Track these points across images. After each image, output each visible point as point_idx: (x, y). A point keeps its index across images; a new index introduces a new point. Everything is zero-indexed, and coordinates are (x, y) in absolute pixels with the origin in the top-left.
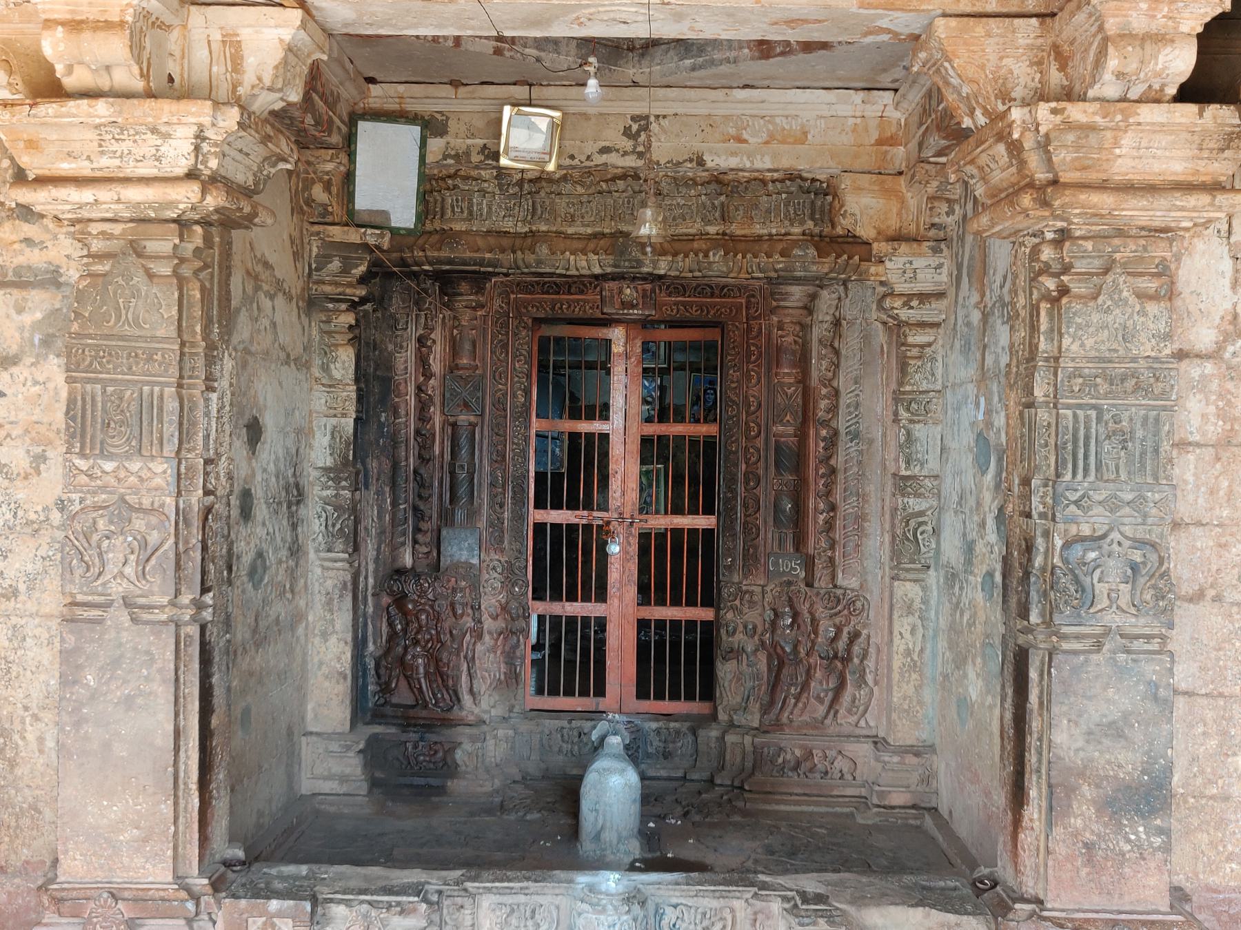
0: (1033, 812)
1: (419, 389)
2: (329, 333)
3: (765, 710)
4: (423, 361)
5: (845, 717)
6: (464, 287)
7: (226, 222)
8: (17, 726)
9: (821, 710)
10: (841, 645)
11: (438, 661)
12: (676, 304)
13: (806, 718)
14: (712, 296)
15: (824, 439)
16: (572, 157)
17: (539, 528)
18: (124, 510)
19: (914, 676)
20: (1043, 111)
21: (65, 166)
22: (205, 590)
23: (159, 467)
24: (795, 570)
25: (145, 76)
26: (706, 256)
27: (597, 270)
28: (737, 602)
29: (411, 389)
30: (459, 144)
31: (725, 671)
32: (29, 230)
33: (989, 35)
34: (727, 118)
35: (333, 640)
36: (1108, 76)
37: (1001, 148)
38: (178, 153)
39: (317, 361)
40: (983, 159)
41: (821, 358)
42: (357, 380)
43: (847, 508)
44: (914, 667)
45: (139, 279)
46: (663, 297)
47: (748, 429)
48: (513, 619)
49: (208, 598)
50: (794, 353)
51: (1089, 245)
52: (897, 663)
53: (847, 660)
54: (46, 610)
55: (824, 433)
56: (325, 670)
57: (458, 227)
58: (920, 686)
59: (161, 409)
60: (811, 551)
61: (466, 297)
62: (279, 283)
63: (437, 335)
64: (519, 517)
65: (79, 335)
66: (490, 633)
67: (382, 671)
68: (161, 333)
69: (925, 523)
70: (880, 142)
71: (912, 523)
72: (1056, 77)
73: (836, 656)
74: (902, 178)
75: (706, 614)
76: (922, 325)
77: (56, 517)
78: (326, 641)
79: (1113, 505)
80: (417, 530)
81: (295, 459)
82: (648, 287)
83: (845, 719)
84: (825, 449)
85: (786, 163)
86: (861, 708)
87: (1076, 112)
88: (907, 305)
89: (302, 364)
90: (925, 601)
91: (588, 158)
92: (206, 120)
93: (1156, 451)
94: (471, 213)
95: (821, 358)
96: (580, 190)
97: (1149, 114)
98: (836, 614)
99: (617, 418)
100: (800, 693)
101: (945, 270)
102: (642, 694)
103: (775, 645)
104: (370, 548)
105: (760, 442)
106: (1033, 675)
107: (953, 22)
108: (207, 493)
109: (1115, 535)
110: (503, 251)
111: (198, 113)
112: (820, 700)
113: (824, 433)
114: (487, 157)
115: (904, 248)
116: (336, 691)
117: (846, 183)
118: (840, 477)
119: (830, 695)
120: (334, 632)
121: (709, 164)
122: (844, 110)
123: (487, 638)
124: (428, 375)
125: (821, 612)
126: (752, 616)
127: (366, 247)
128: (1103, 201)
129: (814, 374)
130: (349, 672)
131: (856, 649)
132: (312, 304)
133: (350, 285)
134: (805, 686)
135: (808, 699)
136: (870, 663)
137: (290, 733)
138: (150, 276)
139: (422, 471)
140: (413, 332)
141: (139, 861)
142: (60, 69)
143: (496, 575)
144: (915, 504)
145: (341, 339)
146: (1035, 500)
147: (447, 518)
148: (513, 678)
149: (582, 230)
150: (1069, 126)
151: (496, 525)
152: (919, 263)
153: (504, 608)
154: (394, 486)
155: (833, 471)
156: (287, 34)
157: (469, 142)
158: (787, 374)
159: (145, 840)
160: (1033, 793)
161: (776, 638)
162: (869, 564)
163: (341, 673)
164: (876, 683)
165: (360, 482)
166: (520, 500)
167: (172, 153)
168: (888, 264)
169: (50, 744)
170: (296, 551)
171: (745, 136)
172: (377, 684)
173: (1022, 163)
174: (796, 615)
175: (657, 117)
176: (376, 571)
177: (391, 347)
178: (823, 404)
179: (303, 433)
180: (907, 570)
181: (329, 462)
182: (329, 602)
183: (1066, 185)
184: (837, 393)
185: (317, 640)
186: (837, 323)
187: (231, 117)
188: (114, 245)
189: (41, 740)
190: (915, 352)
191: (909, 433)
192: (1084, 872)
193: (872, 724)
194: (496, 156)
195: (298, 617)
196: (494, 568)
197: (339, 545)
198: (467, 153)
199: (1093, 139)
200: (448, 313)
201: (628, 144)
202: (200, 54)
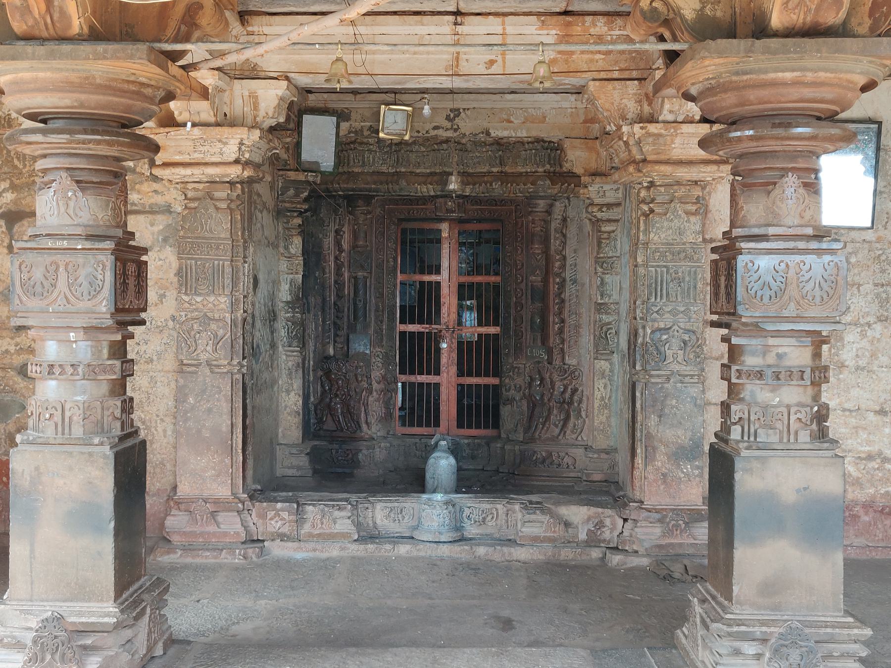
0: (639, 460)
1: (336, 258)
2: (288, 229)
3: (526, 431)
4: (338, 243)
6: (360, 202)
7: (250, 181)
8: (153, 424)
9: (557, 431)
10: (567, 395)
11: (348, 406)
12: (476, 210)
13: (548, 435)
14: (496, 205)
15: (558, 284)
16: (418, 132)
17: (403, 334)
18: (206, 320)
19: (606, 411)
20: (637, 127)
21: (177, 157)
22: (244, 358)
23: (223, 299)
25: (215, 116)
26: (491, 185)
27: (432, 193)
28: (511, 374)
29: (332, 258)
30: (357, 125)
31: (505, 411)
32: (156, 186)
33: (614, 89)
34: (502, 109)
35: (293, 394)
36: (665, 112)
37: (621, 143)
38: (231, 152)
39: (282, 244)
40: (616, 147)
41: (556, 239)
42: (303, 254)
43: (570, 321)
44: (605, 406)
45: (212, 210)
46: (469, 207)
47: (517, 278)
49: (245, 363)
50: (541, 236)
51: (662, 189)
52: (596, 405)
53: (570, 403)
54: (166, 369)
55: (558, 280)
56: (288, 410)
57: (356, 170)
58: (610, 417)
59: (223, 272)
60: (551, 345)
61: (362, 208)
62: (264, 204)
63: (345, 229)
64: (392, 328)
65: (183, 237)
66: (376, 391)
67: (318, 412)
68: (223, 236)
69: (611, 328)
70: (585, 122)
71: (604, 329)
72: (647, 109)
73: (564, 402)
74: (598, 142)
75: (494, 381)
76: (609, 221)
77: (171, 324)
79: (674, 313)
80: (336, 335)
81: (272, 297)
82: (461, 201)
83: (570, 436)
84: (558, 289)
85: (534, 133)
87: (653, 128)
88: (600, 210)
89: (275, 246)
90: (611, 371)
91: (427, 132)
92: (245, 136)
93: (695, 287)
94: (364, 162)
95: (556, 239)
96: (423, 149)
97: (686, 128)
99: (445, 273)
100: (545, 422)
101: (620, 191)
102: (460, 425)
103: (531, 395)
104: (311, 345)
105: (523, 286)
106: (638, 394)
107: (597, 83)
108: (245, 312)
109: (676, 327)
110: (381, 183)
111: (241, 133)
112: (557, 426)
113: (558, 280)
114: (372, 132)
115: (598, 179)
117: (567, 144)
118: (567, 304)
119: (562, 423)
121: (493, 135)
122: (565, 104)
123: (375, 393)
124: (341, 250)
125: (556, 377)
126: (519, 381)
127: (308, 182)
128: (667, 169)
129: (553, 248)
130: (301, 411)
131: (576, 398)
132: (279, 213)
133: (299, 203)
134: (548, 418)
136: (584, 406)
137: (272, 443)
138: (217, 209)
139: (338, 303)
140: (333, 227)
141: (215, 486)
142: (176, 114)
144: (605, 318)
145: (294, 232)
146: (638, 311)
147: (352, 328)
148: (389, 415)
149: (424, 171)
150: (649, 135)
151: (379, 332)
152: (606, 187)
154: (323, 310)
155: (563, 301)
156: (280, 93)
157: (362, 124)
158: (537, 248)
159: (218, 476)
160: (639, 451)
162: (582, 351)
165: (305, 309)
166: (392, 319)
167: (228, 151)
168: (590, 189)
169: (169, 433)
170: (273, 346)
171: (512, 119)
173: (630, 151)
174: (542, 380)
175: (464, 109)
176: (314, 357)
177: (321, 236)
178: (557, 264)
179: (276, 283)
180: (602, 354)
181: (289, 298)
182: (290, 374)
183: (650, 162)
184: (564, 258)
185: (284, 394)
186: (564, 220)
187: (257, 133)
188: (199, 194)
189: (165, 431)
190: (605, 236)
191: (602, 280)
192: (662, 487)
194: (377, 132)
195: (274, 382)
197: (295, 343)
198: (362, 130)
199: (661, 140)
200: (351, 217)
201: (449, 125)
202: (239, 102)
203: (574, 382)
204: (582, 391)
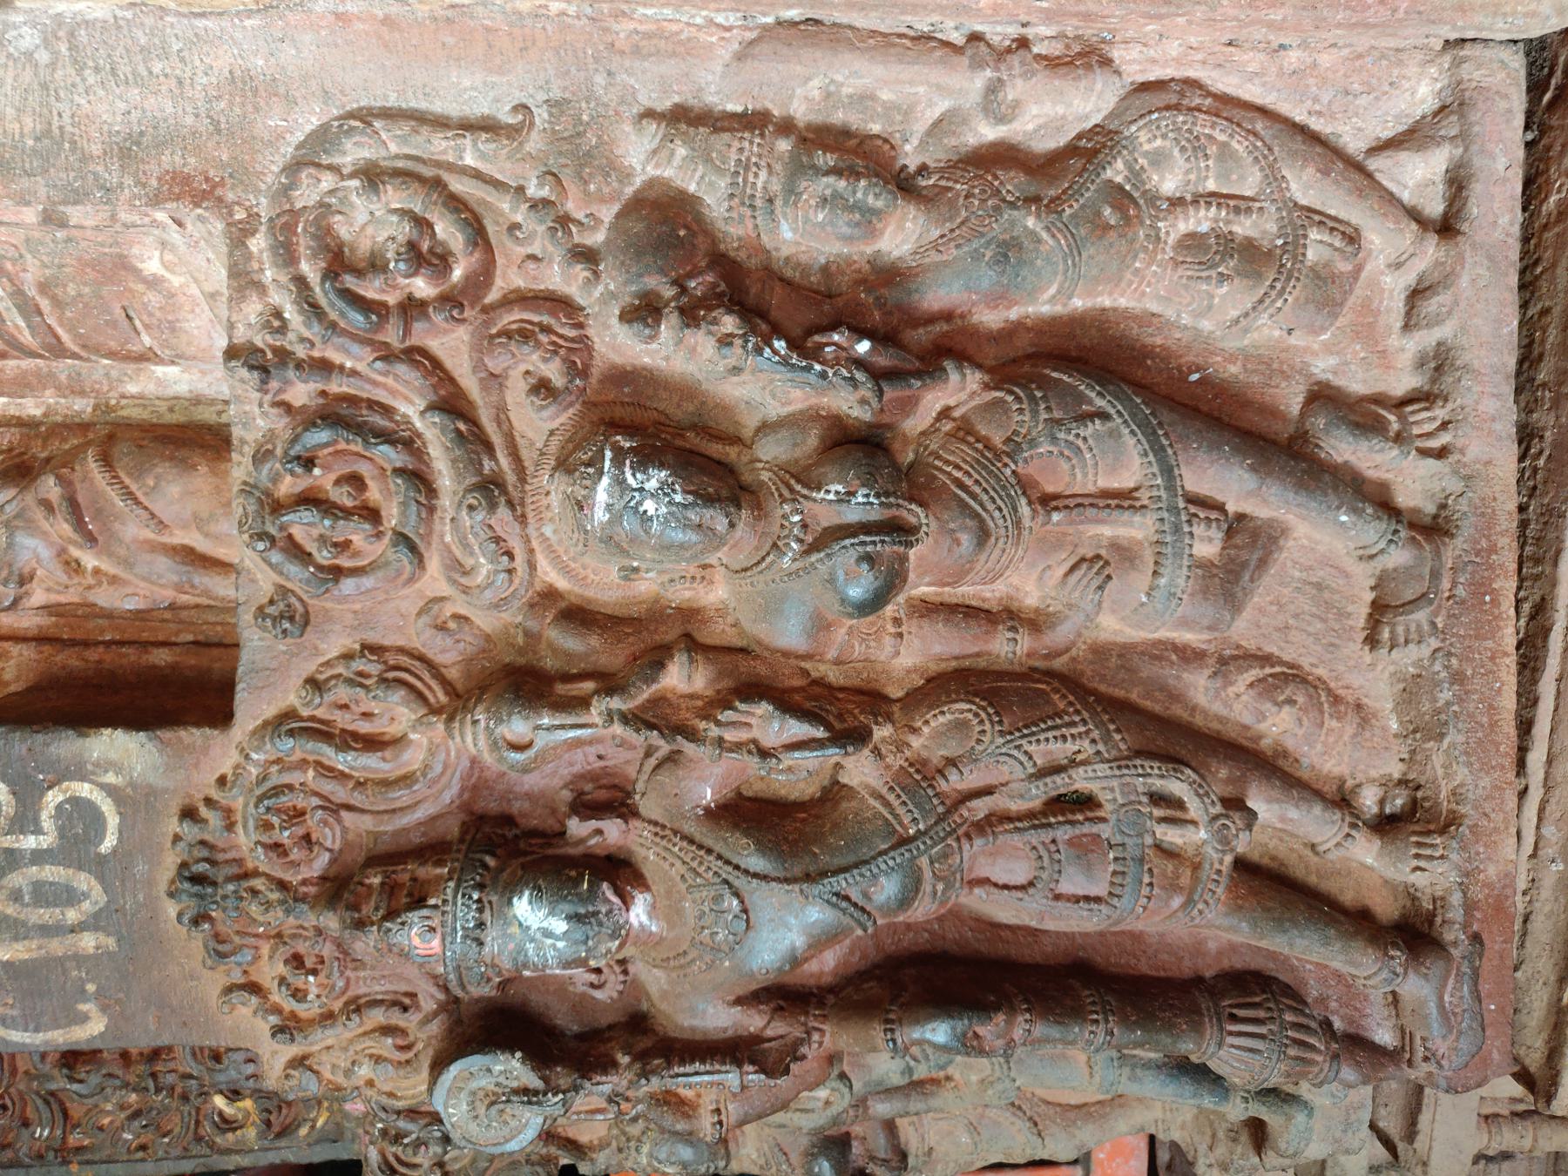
5: (1366, 331)
9: (1325, 545)
24: (81, 817)
86: (1305, 185)
98: (472, 440)
131: (804, 232)
135: (1228, 662)
161: (717, 1017)
164: (1088, 57)
193: (1421, 92)
203: (531, 262)
204: (685, 119)
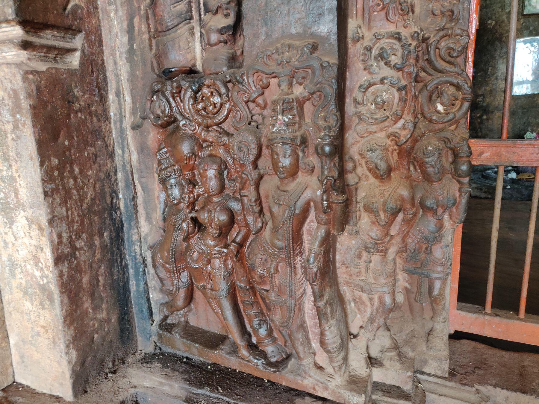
35: (21, 221)
48: (427, 178)
56: (20, 278)
78: (12, 222)
116: (42, 322)
120: (19, 205)
123: (364, 221)
130: (54, 288)
143: (387, 72)
153: (408, 153)
163: (43, 288)
172: (161, 290)
176: (132, 78)
196: (382, 56)
